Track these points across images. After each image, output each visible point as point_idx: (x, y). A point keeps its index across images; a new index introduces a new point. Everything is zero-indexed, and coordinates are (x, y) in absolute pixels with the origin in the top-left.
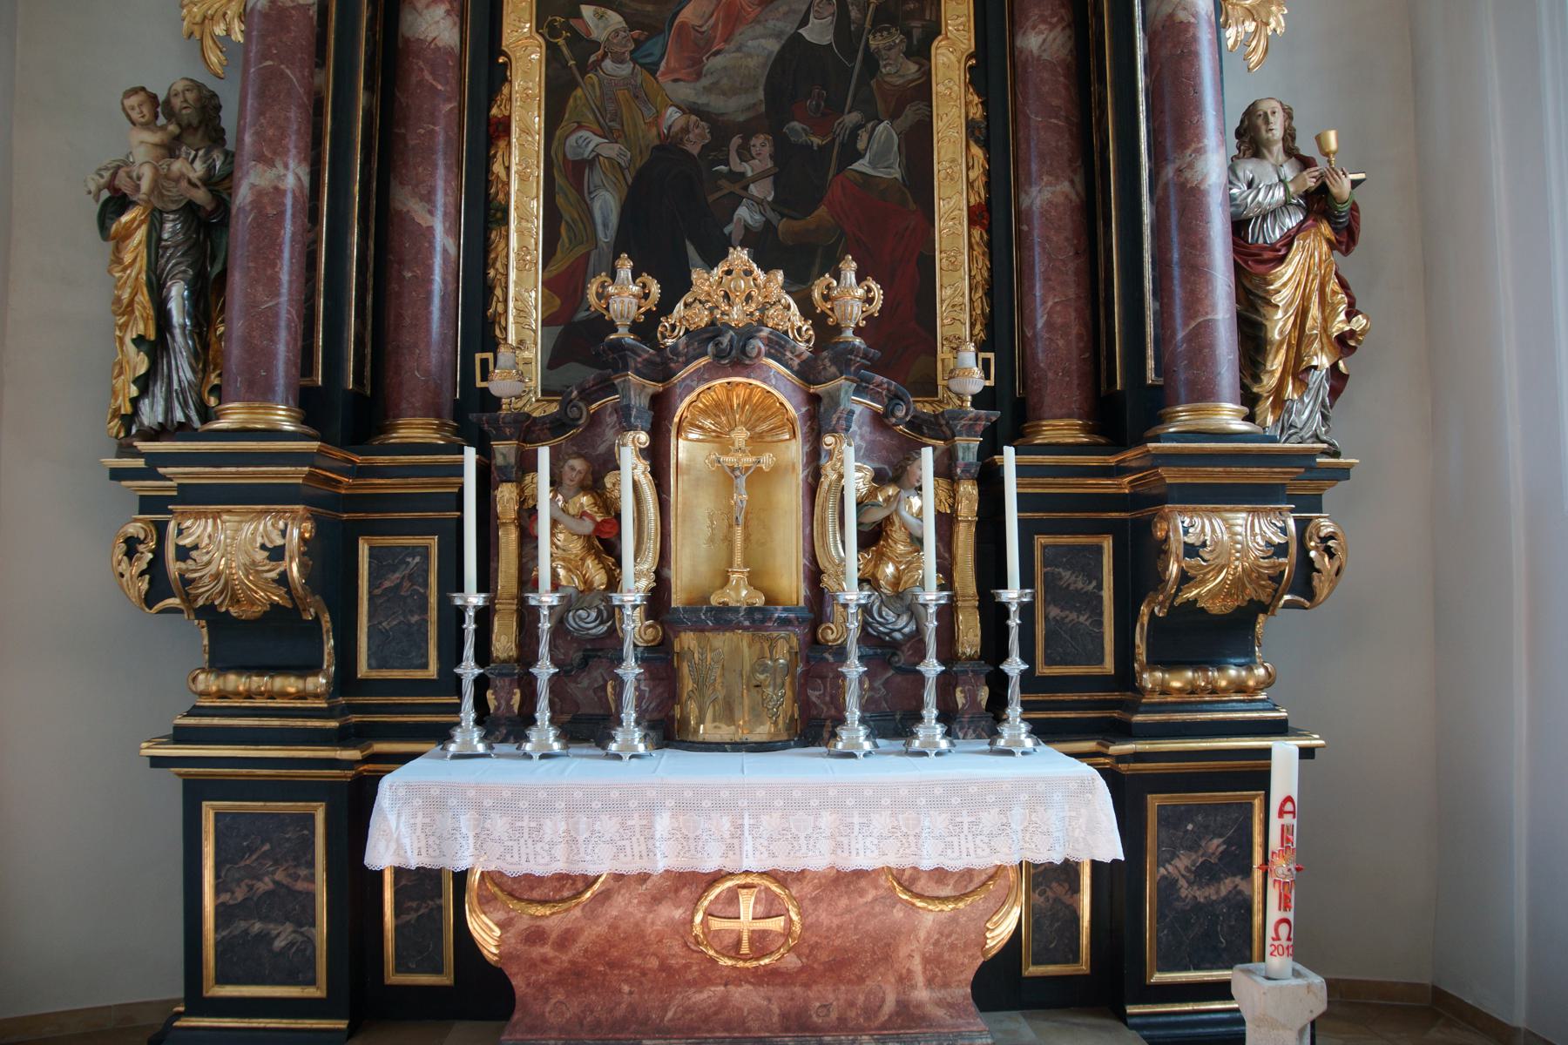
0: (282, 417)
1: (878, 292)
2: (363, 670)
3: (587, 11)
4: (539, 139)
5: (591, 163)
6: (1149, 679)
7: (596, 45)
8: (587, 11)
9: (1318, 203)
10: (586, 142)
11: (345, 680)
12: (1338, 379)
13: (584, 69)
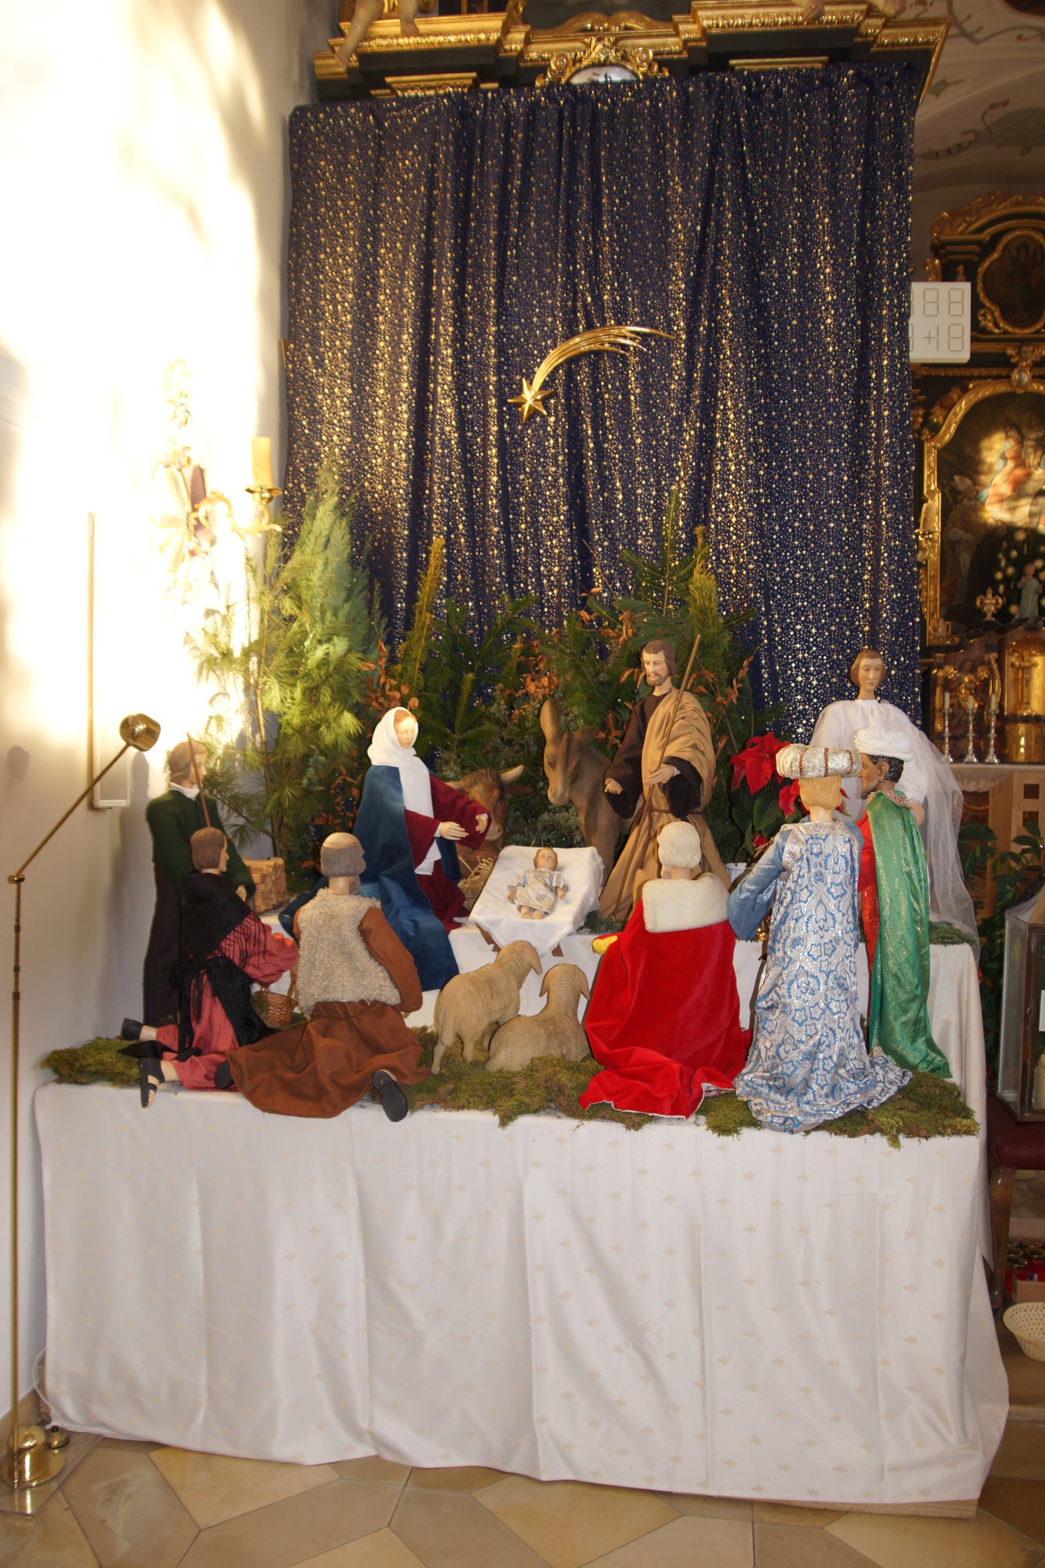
3: (957, 478)
5: (959, 542)
7: (959, 493)
8: (957, 478)
10: (958, 533)
13: (956, 502)
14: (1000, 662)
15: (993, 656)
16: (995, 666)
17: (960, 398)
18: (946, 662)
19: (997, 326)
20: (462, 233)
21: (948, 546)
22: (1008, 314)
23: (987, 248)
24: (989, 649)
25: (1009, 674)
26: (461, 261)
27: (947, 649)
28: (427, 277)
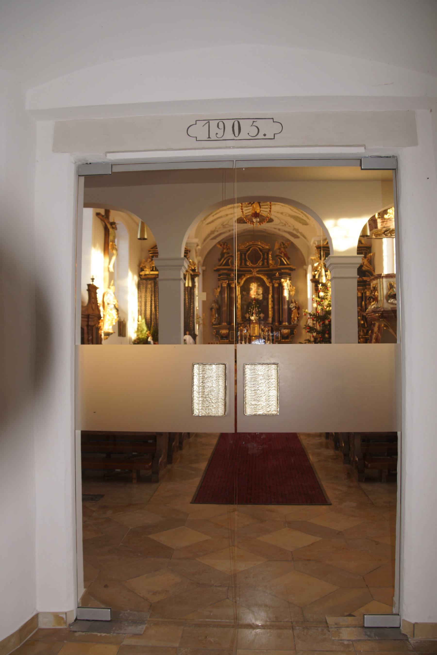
0: (226, 324)
1: (264, 315)
2: (230, 340)
4: (240, 302)
6: (281, 340)
9: (296, 307)
10: (244, 302)
11: (229, 341)
12: (298, 320)
14: (250, 326)
15: (248, 325)
16: (249, 327)
17: (244, 278)
18: (241, 326)
19: (250, 264)
20: (155, 293)
21: (242, 305)
22: (252, 262)
23: (248, 251)
24: (248, 324)
25: (252, 328)
26: (155, 295)
27: (241, 324)
28: (151, 297)
